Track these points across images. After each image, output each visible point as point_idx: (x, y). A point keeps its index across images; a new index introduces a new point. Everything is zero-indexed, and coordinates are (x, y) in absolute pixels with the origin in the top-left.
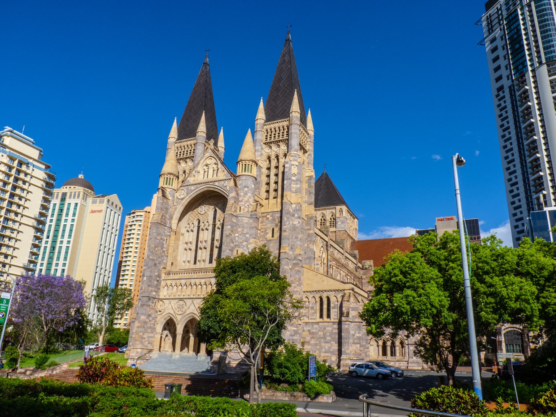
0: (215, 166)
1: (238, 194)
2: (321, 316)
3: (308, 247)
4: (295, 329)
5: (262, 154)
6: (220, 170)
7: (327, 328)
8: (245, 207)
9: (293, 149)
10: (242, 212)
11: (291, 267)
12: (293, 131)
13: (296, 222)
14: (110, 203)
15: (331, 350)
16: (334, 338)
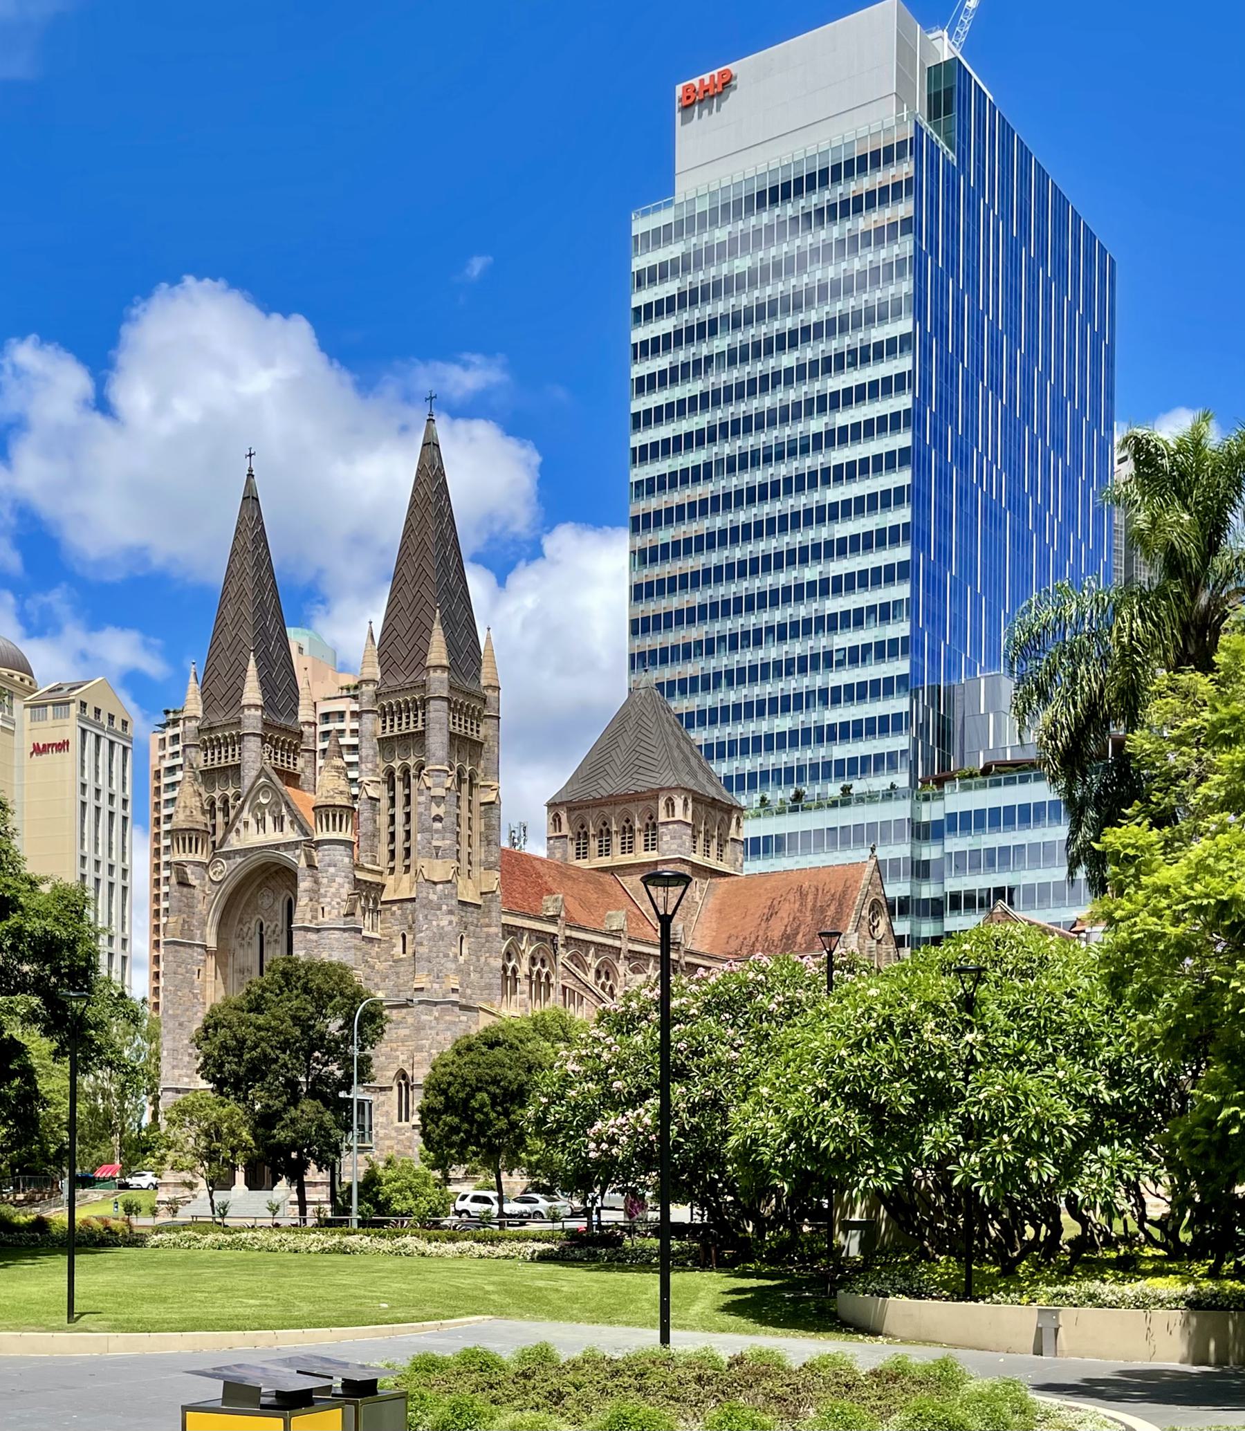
1: (316, 882)
3: (486, 963)
5: (377, 766)
8: (333, 908)
9: (433, 760)
10: (326, 919)
11: (437, 1014)
12: (432, 715)
13: (444, 923)
14: (90, 713)
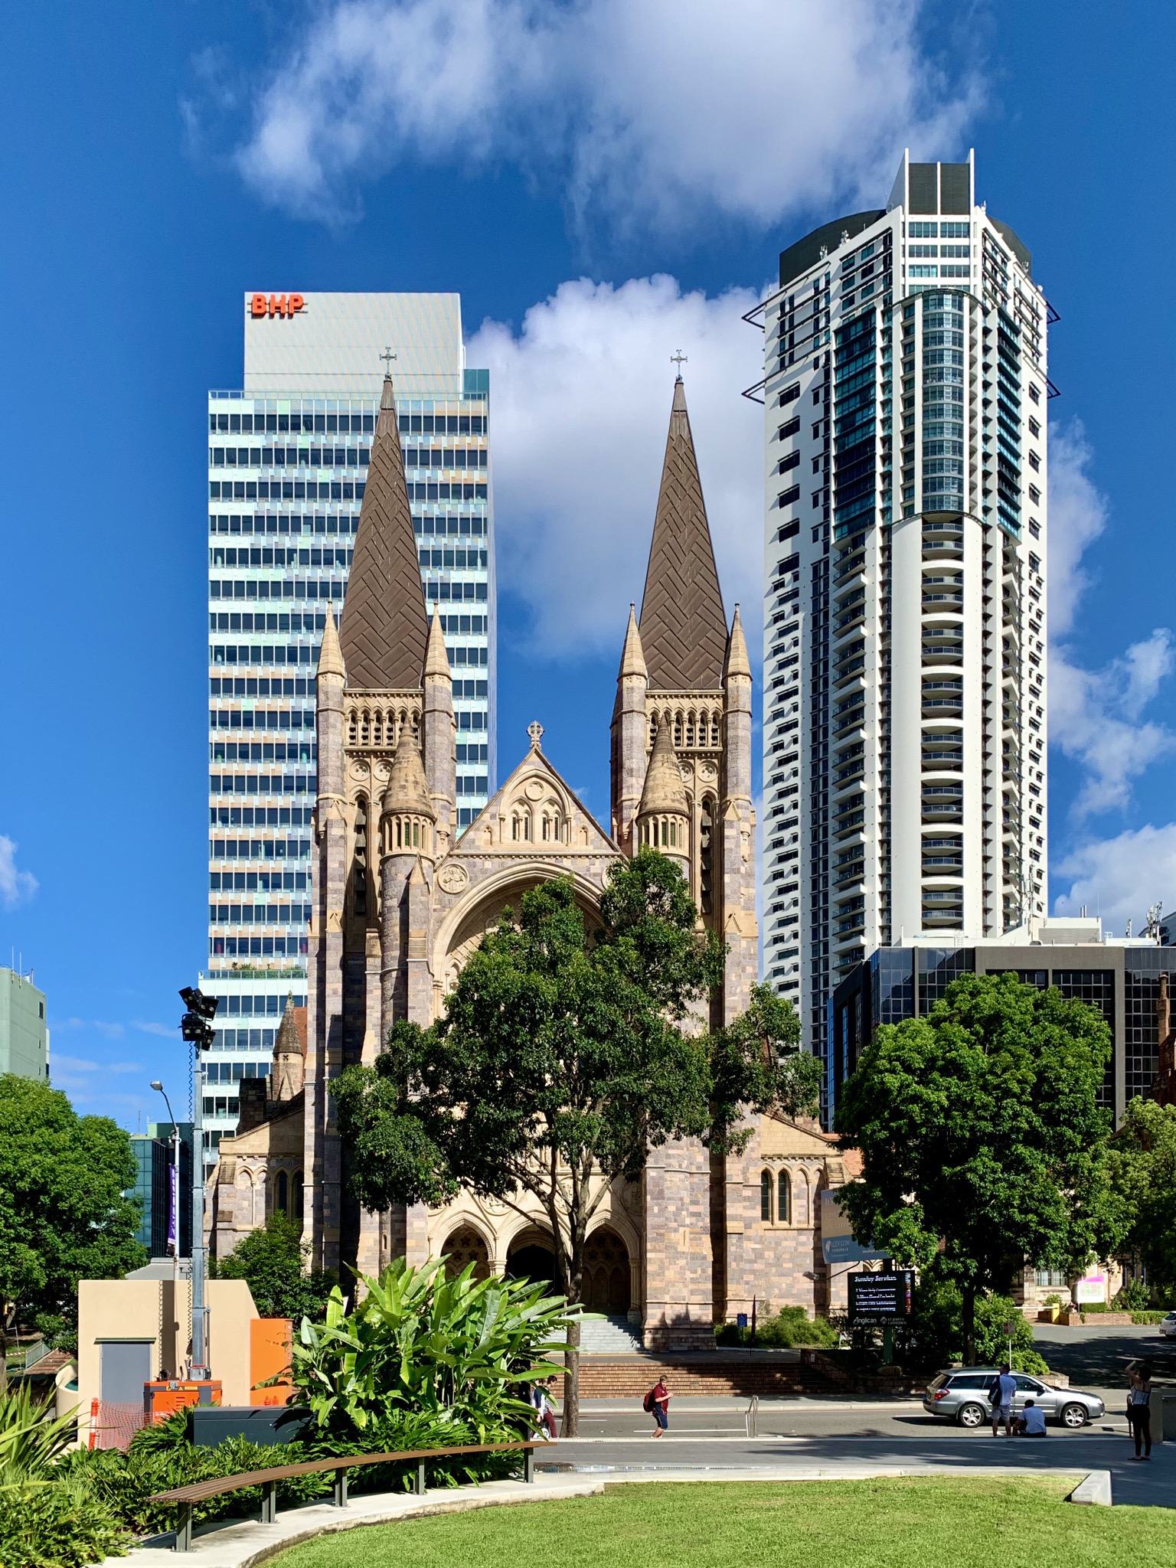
0: (552, 811)
2: (765, 1216)
4: (757, 1246)
6: (573, 823)
7: (784, 1244)
15: (795, 1291)
16: (800, 1265)
